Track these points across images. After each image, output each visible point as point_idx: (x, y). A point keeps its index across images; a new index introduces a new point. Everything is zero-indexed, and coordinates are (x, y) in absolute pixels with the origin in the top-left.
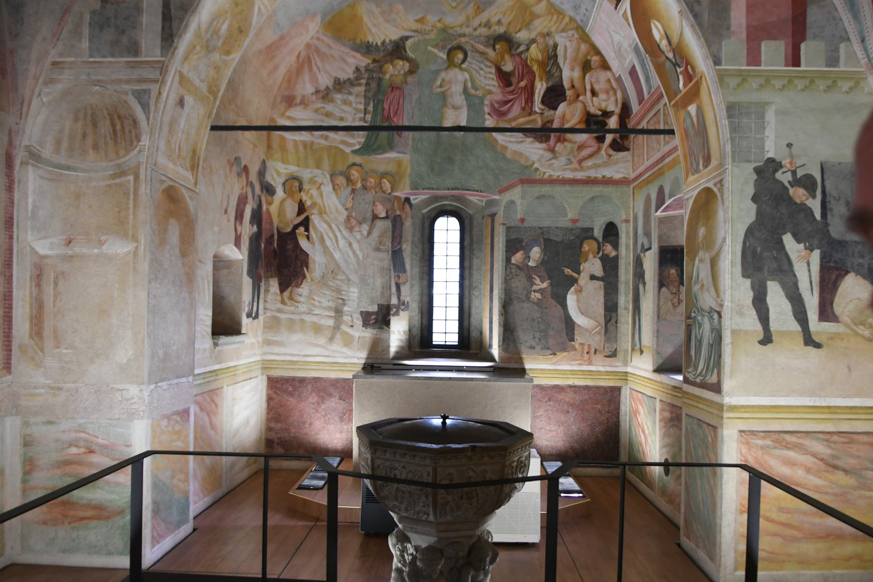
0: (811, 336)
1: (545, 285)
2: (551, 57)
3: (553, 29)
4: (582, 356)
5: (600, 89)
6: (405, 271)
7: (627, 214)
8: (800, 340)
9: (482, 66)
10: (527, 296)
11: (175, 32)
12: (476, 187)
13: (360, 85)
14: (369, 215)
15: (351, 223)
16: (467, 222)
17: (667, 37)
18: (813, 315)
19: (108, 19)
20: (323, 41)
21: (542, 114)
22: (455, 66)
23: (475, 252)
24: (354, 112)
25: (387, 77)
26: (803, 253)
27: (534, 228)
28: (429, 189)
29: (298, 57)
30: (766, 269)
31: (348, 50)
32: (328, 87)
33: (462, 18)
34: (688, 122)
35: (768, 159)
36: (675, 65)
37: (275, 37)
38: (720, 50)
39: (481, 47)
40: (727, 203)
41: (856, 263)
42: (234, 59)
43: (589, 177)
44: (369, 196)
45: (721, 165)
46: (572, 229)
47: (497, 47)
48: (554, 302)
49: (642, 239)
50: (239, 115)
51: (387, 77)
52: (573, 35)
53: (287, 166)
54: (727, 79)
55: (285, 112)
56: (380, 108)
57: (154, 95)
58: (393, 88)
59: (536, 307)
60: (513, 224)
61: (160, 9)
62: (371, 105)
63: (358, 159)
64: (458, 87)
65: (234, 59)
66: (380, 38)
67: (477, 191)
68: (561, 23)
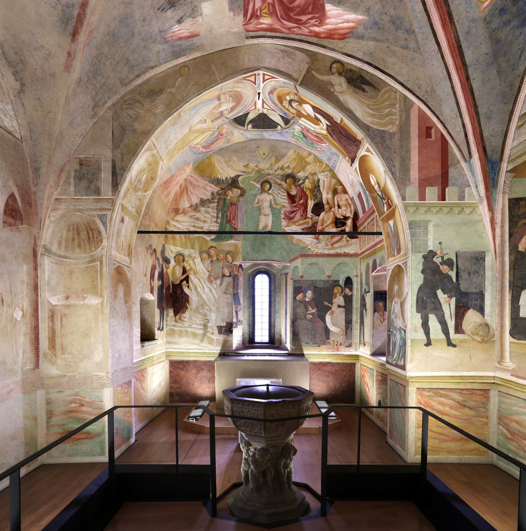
0: (451, 341)
1: (314, 311)
2: (316, 187)
3: (317, 171)
4: (334, 347)
5: (342, 204)
6: (240, 304)
7: (357, 272)
8: (445, 343)
9: (280, 192)
10: (304, 317)
11: (118, 182)
12: (277, 259)
13: (214, 202)
14: (220, 275)
15: (211, 279)
16: (272, 277)
17: (378, 184)
18: (452, 331)
19: (84, 174)
20: (194, 177)
21: (312, 218)
22: (265, 192)
23: (277, 294)
24: (211, 217)
25: (229, 198)
26: (447, 299)
27: (308, 281)
28: (252, 260)
29: (181, 186)
30: (428, 308)
31: (207, 183)
32: (197, 204)
33: (268, 165)
34: (389, 229)
35: (430, 250)
36: (382, 198)
37: (169, 177)
38: (405, 192)
39: (279, 181)
40: (409, 274)
41: (473, 303)
42: (149, 194)
43: (337, 253)
44: (221, 264)
45: (406, 254)
46: (328, 281)
47: (288, 181)
48: (319, 320)
49: (365, 286)
50: (151, 221)
51: (229, 198)
52: (328, 174)
53: (176, 248)
54: (409, 208)
55: (174, 217)
56: (225, 215)
57: (109, 217)
58: (232, 204)
59: (309, 322)
60: (297, 279)
61: (111, 169)
62: (220, 214)
63: (214, 244)
64: (267, 204)
65: (149, 194)
66: (225, 176)
67: (278, 261)
68: (321, 167)
